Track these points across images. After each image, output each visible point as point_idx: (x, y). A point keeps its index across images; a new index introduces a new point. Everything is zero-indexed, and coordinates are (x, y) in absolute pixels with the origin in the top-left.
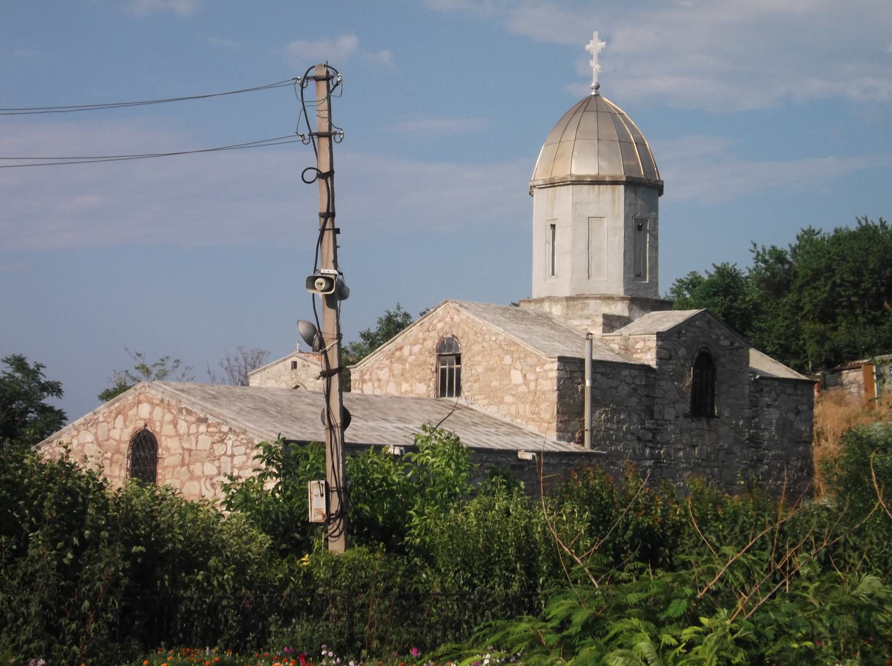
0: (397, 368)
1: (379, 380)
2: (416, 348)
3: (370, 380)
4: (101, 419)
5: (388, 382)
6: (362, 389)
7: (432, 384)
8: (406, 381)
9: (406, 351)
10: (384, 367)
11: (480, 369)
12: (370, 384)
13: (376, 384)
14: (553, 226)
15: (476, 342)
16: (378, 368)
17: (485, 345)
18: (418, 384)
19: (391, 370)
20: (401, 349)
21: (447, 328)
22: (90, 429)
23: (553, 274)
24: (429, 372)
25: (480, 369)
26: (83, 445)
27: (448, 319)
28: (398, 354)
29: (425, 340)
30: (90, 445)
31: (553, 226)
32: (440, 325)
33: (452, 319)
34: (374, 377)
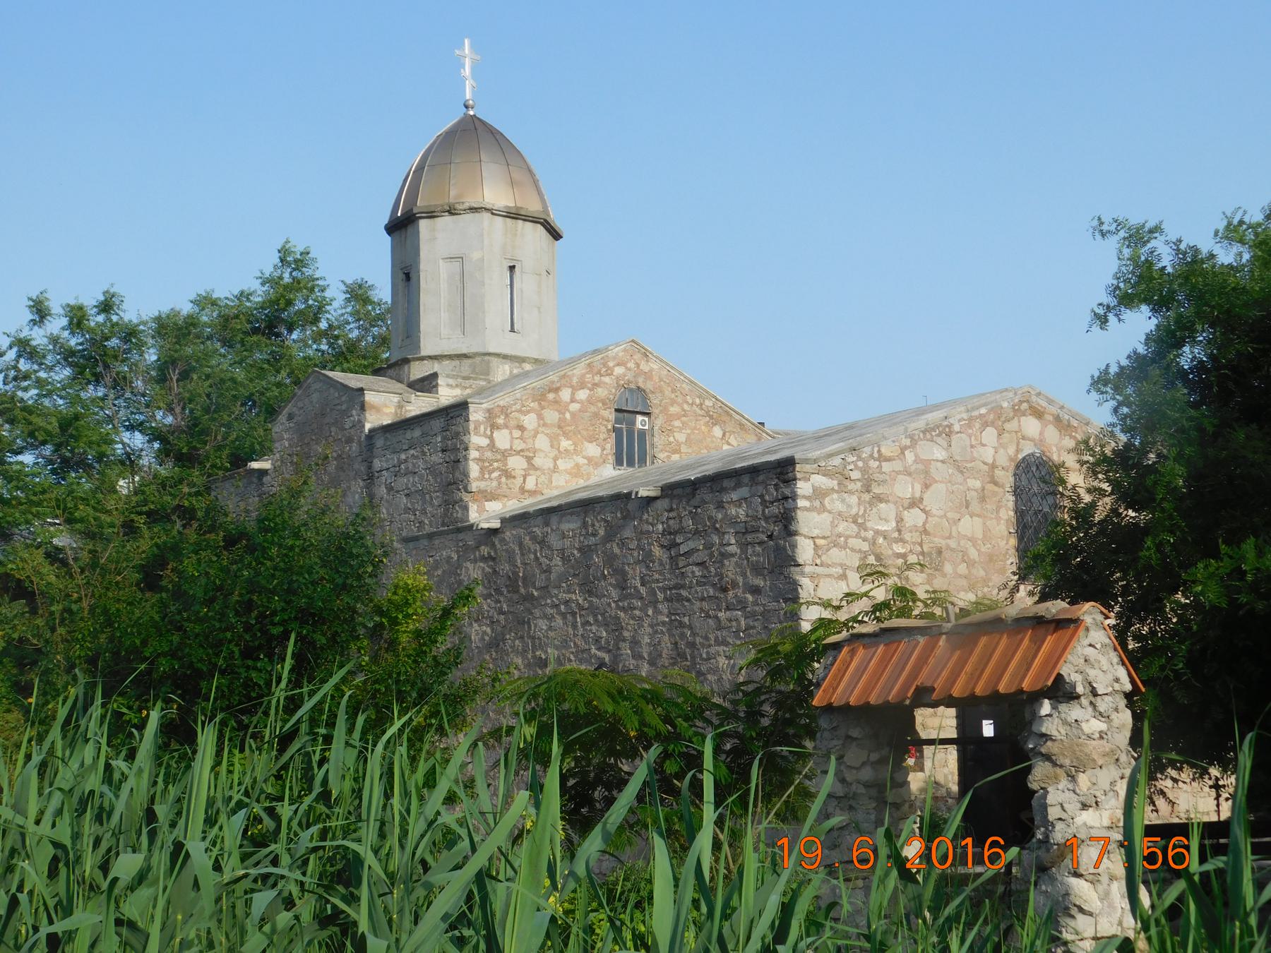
0: (551, 416)
1: (521, 428)
2: (582, 395)
3: (506, 427)
4: (957, 428)
5: (536, 433)
6: (491, 438)
7: (608, 446)
8: (566, 435)
9: (565, 394)
10: (529, 412)
11: (681, 437)
12: (505, 432)
13: (517, 433)
14: (512, 268)
15: (673, 402)
16: (520, 411)
17: (686, 407)
18: (586, 444)
19: (540, 417)
20: (557, 390)
21: (629, 376)
22: (939, 440)
23: (512, 330)
24: (603, 429)
25: (681, 437)
26: (927, 463)
27: (631, 365)
28: (551, 396)
29: (596, 385)
30: (939, 464)
31: (512, 268)
32: (619, 371)
33: (638, 365)
34: (512, 423)
